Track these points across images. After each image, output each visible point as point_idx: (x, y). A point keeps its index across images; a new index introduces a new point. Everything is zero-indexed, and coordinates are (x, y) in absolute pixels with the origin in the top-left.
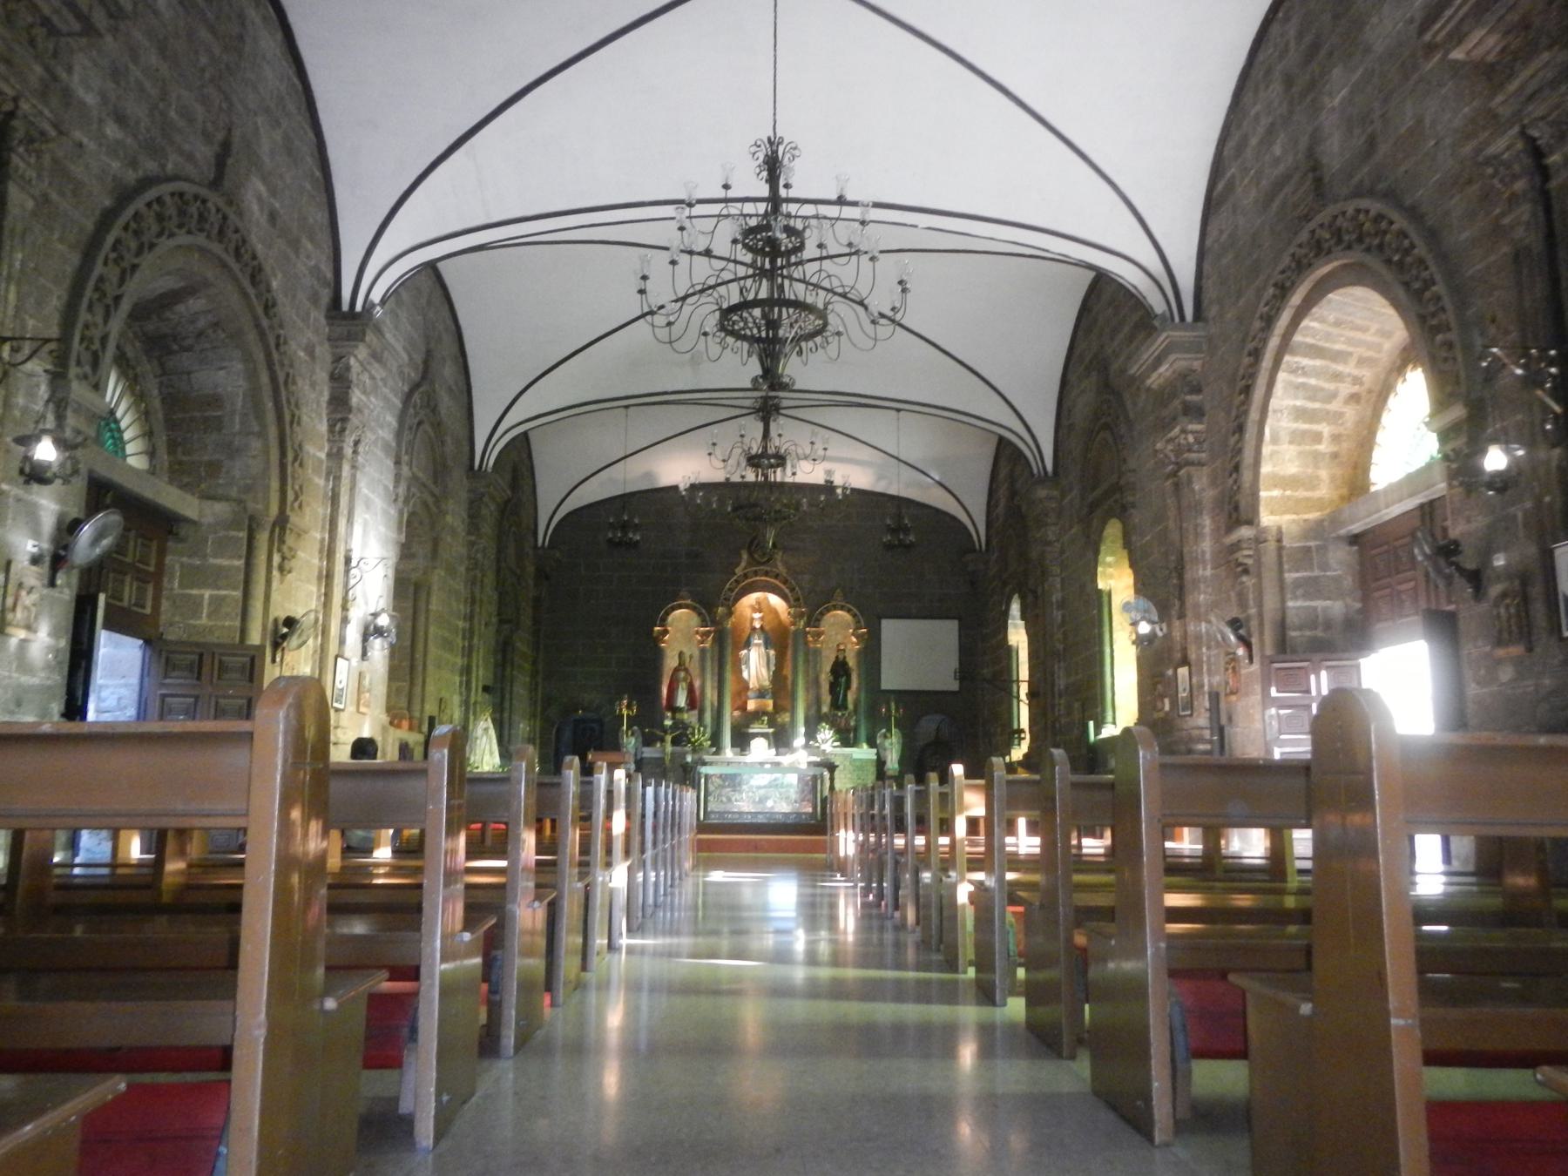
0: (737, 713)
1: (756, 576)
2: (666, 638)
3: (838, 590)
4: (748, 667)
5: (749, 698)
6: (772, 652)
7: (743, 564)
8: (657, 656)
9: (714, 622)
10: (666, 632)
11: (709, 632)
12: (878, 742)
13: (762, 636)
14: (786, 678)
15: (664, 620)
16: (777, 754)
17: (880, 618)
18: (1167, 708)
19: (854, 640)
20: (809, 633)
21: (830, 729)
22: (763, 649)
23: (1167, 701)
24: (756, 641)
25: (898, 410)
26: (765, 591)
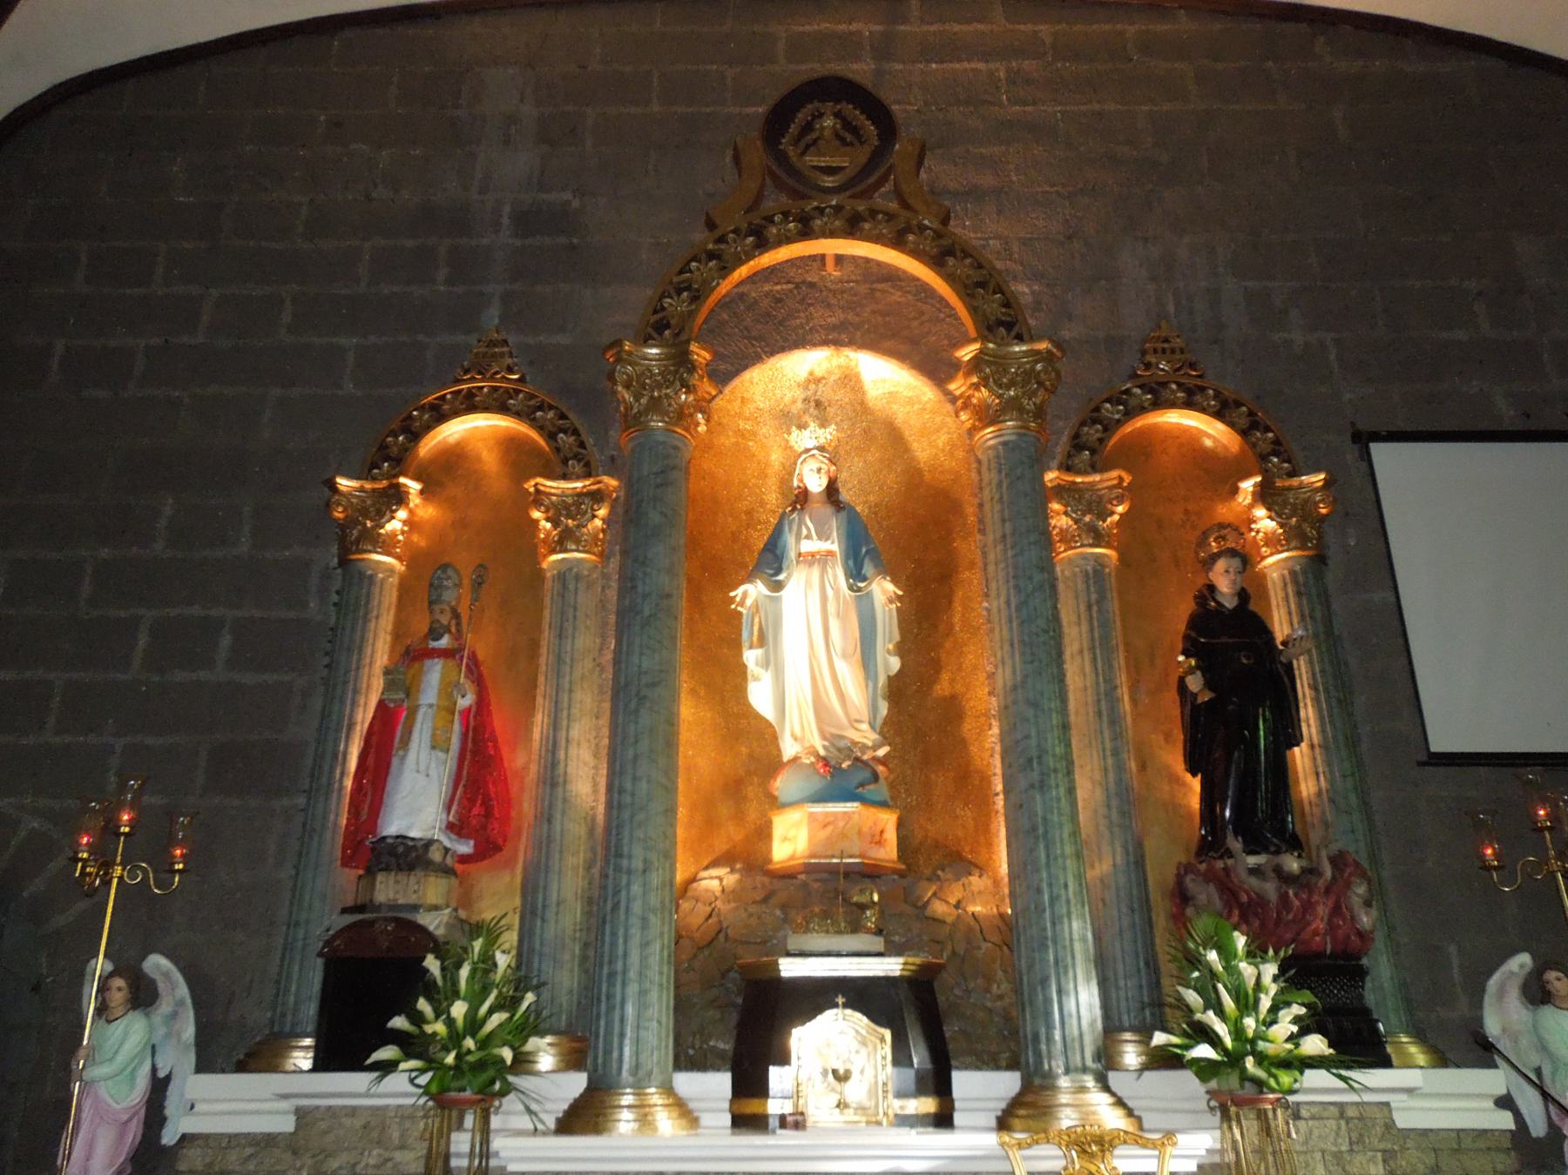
0: (716, 881)
4: (773, 662)
5: (776, 804)
6: (883, 590)
10: (399, 497)
11: (597, 497)
12: (1492, 1026)
13: (834, 524)
14: (953, 710)
16: (943, 1119)
17: (1363, 439)
19: (1264, 522)
20: (1061, 491)
21: (1255, 953)
22: (838, 574)
24: (807, 546)
26: (837, 343)
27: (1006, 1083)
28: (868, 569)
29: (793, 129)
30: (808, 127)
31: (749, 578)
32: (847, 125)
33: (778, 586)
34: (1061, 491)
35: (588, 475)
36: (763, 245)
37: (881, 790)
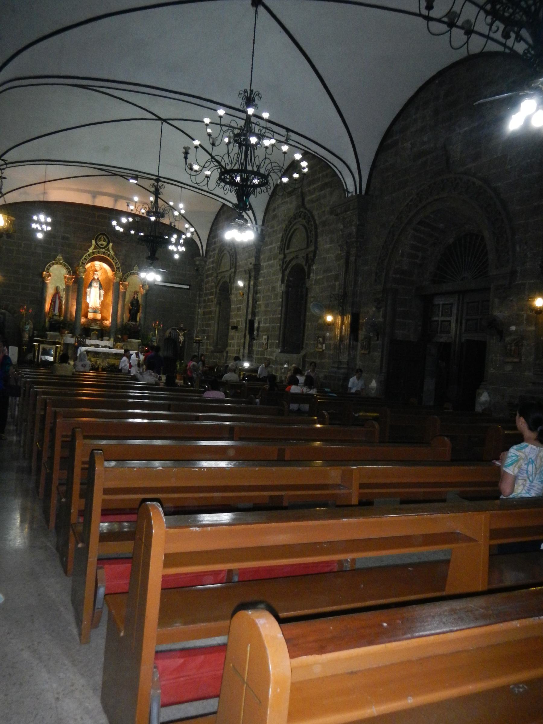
1: (99, 254)
2: (49, 278)
3: (136, 265)
4: (90, 297)
6: (102, 292)
7: (93, 247)
8: (44, 286)
9: (75, 273)
10: (49, 275)
11: (72, 278)
15: (48, 269)
18: (324, 349)
22: (98, 289)
23: (324, 345)
25: (182, 187)
27: (108, 338)
28: (101, 288)
29: (98, 239)
30: (100, 238)
31: (88, 288)
32: (105, 239)
33: (91, 289)
34: (122, 284)
35: (71, 275)
36: (94, 254)
37: (100, 312)
